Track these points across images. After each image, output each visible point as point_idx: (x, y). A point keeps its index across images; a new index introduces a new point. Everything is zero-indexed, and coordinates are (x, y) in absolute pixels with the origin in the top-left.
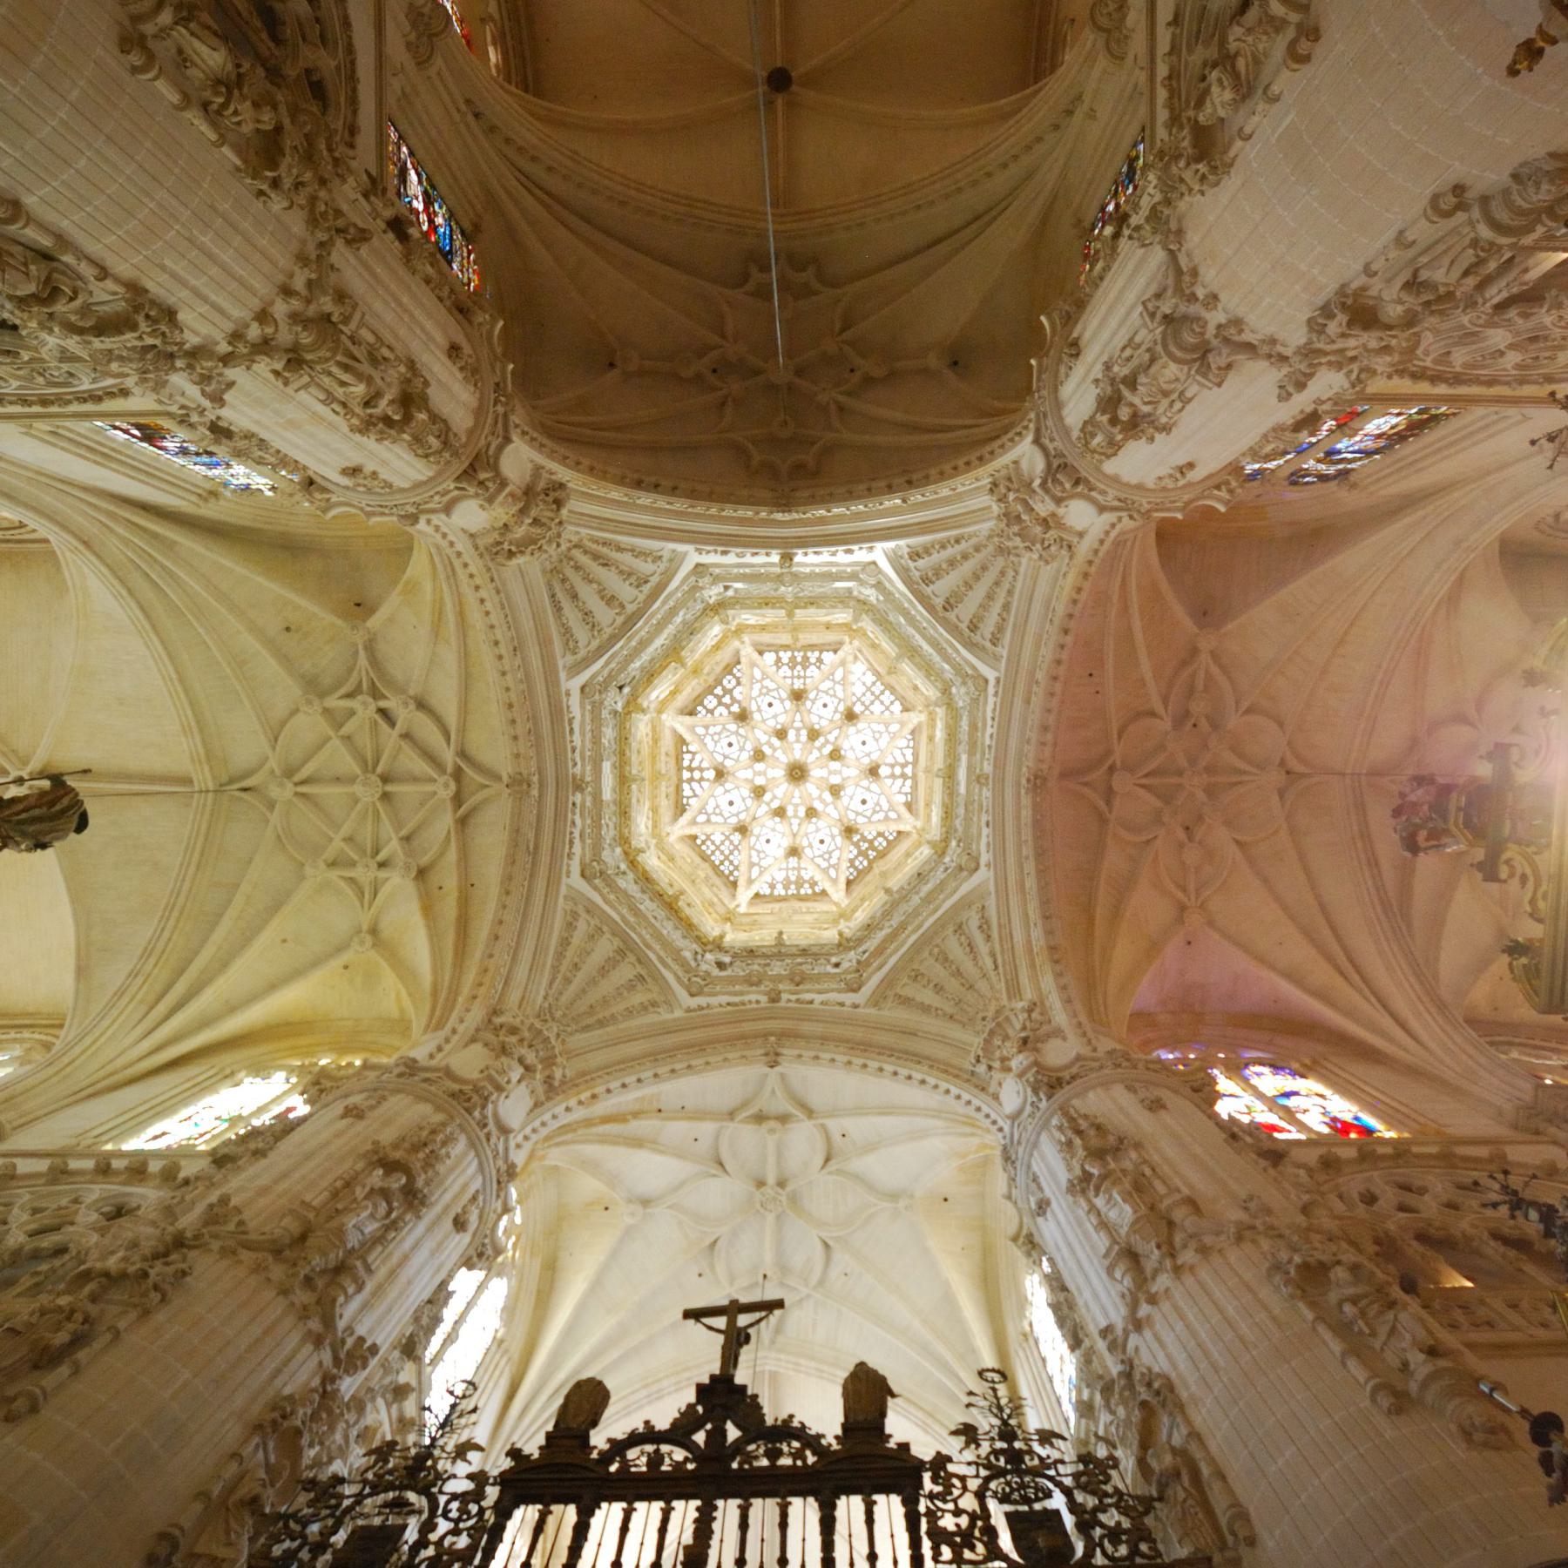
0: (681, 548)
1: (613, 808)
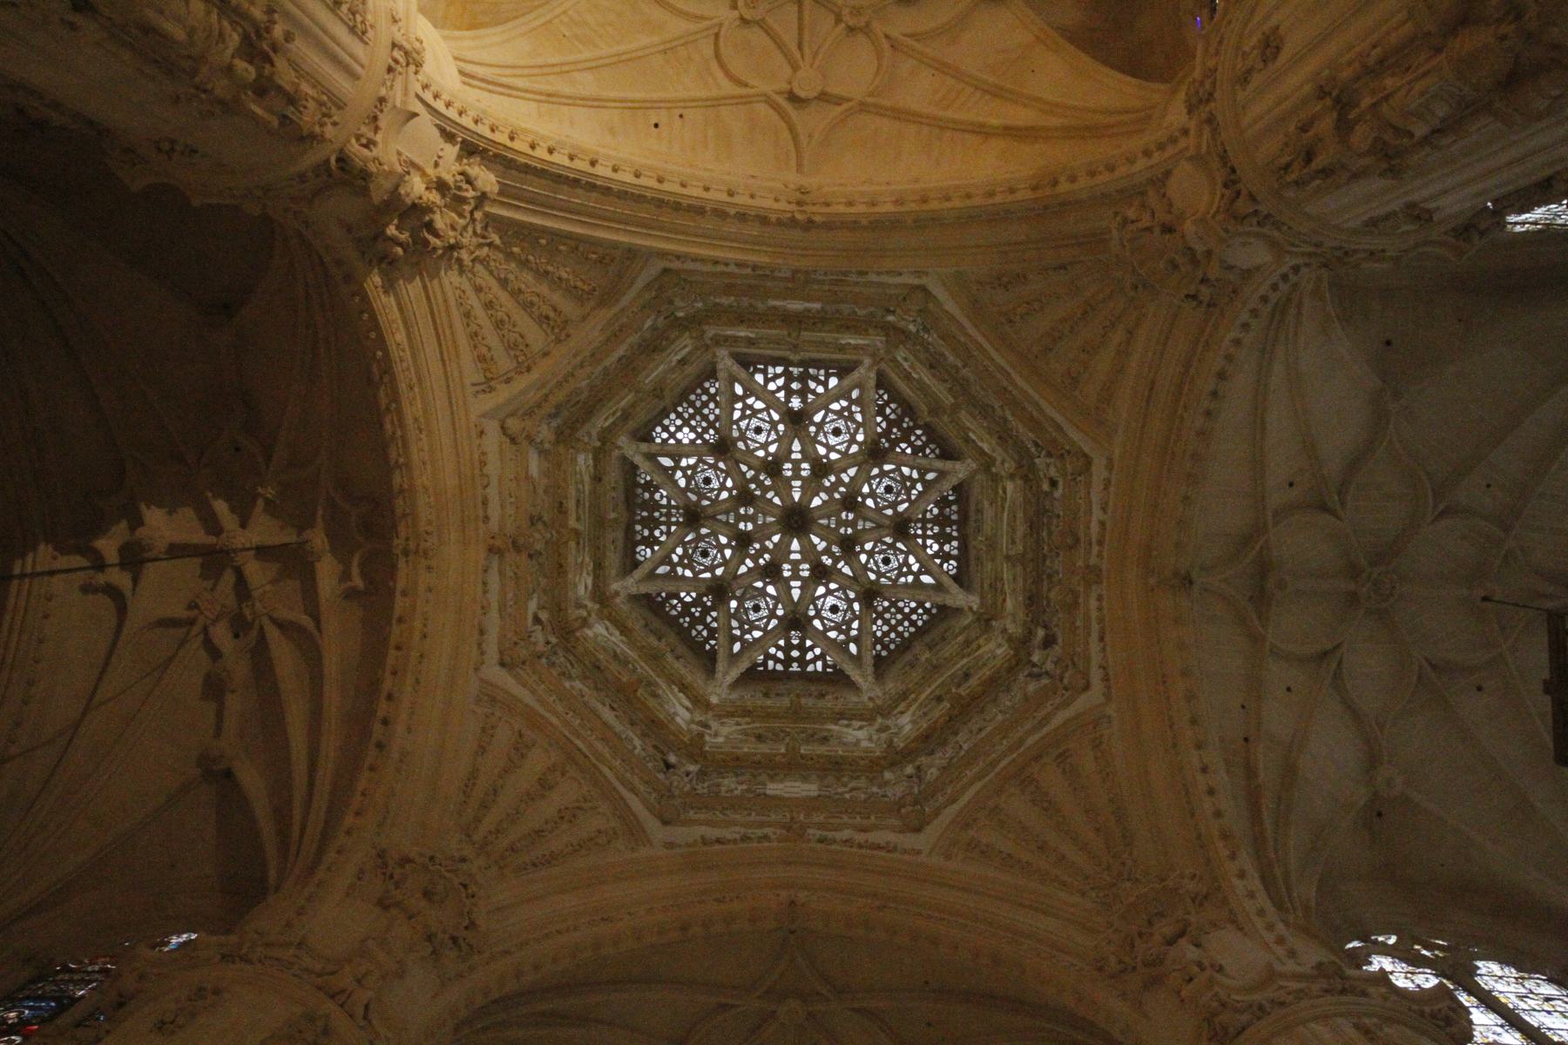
1: (830, 779)
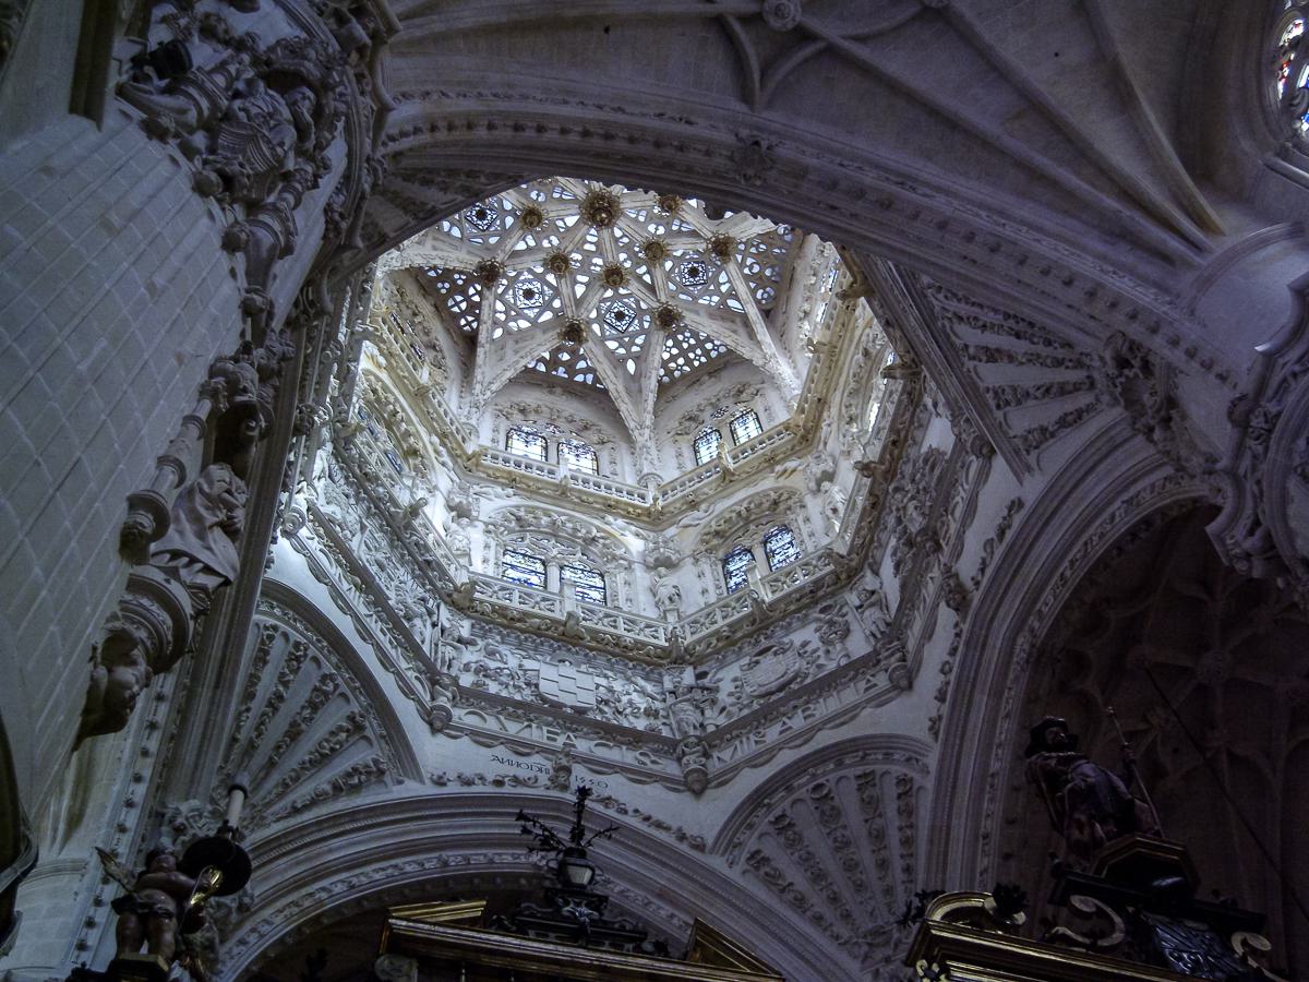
0: (1033, 487)
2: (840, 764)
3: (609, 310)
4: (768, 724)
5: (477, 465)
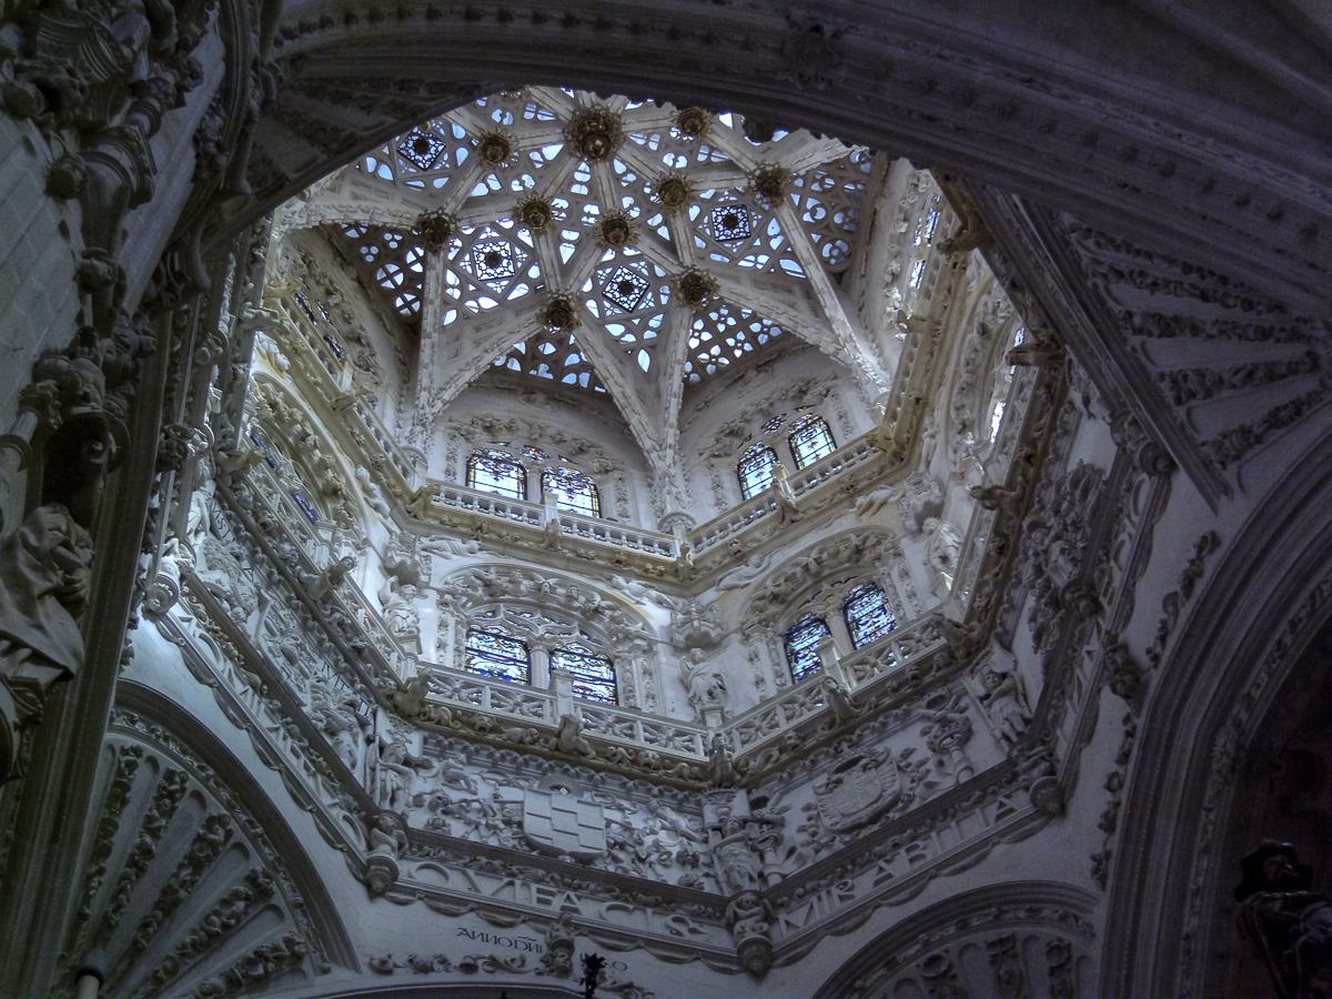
0: (1232, 518)
2: (964, 926)
3: (609, 280)
4: (858, 870)
5: (426, 507)
